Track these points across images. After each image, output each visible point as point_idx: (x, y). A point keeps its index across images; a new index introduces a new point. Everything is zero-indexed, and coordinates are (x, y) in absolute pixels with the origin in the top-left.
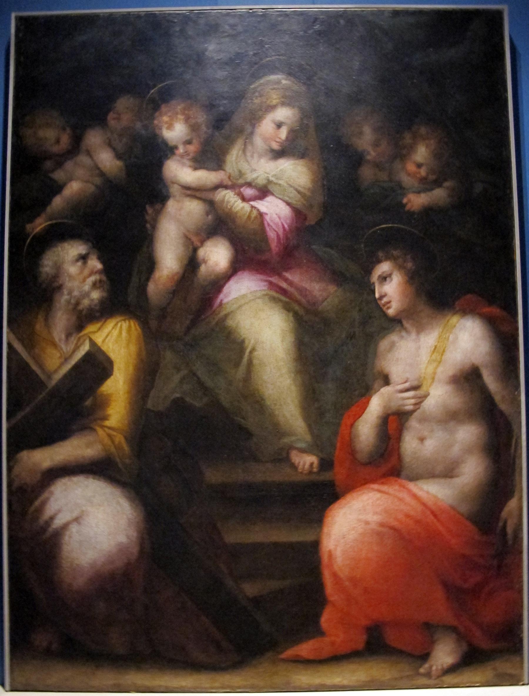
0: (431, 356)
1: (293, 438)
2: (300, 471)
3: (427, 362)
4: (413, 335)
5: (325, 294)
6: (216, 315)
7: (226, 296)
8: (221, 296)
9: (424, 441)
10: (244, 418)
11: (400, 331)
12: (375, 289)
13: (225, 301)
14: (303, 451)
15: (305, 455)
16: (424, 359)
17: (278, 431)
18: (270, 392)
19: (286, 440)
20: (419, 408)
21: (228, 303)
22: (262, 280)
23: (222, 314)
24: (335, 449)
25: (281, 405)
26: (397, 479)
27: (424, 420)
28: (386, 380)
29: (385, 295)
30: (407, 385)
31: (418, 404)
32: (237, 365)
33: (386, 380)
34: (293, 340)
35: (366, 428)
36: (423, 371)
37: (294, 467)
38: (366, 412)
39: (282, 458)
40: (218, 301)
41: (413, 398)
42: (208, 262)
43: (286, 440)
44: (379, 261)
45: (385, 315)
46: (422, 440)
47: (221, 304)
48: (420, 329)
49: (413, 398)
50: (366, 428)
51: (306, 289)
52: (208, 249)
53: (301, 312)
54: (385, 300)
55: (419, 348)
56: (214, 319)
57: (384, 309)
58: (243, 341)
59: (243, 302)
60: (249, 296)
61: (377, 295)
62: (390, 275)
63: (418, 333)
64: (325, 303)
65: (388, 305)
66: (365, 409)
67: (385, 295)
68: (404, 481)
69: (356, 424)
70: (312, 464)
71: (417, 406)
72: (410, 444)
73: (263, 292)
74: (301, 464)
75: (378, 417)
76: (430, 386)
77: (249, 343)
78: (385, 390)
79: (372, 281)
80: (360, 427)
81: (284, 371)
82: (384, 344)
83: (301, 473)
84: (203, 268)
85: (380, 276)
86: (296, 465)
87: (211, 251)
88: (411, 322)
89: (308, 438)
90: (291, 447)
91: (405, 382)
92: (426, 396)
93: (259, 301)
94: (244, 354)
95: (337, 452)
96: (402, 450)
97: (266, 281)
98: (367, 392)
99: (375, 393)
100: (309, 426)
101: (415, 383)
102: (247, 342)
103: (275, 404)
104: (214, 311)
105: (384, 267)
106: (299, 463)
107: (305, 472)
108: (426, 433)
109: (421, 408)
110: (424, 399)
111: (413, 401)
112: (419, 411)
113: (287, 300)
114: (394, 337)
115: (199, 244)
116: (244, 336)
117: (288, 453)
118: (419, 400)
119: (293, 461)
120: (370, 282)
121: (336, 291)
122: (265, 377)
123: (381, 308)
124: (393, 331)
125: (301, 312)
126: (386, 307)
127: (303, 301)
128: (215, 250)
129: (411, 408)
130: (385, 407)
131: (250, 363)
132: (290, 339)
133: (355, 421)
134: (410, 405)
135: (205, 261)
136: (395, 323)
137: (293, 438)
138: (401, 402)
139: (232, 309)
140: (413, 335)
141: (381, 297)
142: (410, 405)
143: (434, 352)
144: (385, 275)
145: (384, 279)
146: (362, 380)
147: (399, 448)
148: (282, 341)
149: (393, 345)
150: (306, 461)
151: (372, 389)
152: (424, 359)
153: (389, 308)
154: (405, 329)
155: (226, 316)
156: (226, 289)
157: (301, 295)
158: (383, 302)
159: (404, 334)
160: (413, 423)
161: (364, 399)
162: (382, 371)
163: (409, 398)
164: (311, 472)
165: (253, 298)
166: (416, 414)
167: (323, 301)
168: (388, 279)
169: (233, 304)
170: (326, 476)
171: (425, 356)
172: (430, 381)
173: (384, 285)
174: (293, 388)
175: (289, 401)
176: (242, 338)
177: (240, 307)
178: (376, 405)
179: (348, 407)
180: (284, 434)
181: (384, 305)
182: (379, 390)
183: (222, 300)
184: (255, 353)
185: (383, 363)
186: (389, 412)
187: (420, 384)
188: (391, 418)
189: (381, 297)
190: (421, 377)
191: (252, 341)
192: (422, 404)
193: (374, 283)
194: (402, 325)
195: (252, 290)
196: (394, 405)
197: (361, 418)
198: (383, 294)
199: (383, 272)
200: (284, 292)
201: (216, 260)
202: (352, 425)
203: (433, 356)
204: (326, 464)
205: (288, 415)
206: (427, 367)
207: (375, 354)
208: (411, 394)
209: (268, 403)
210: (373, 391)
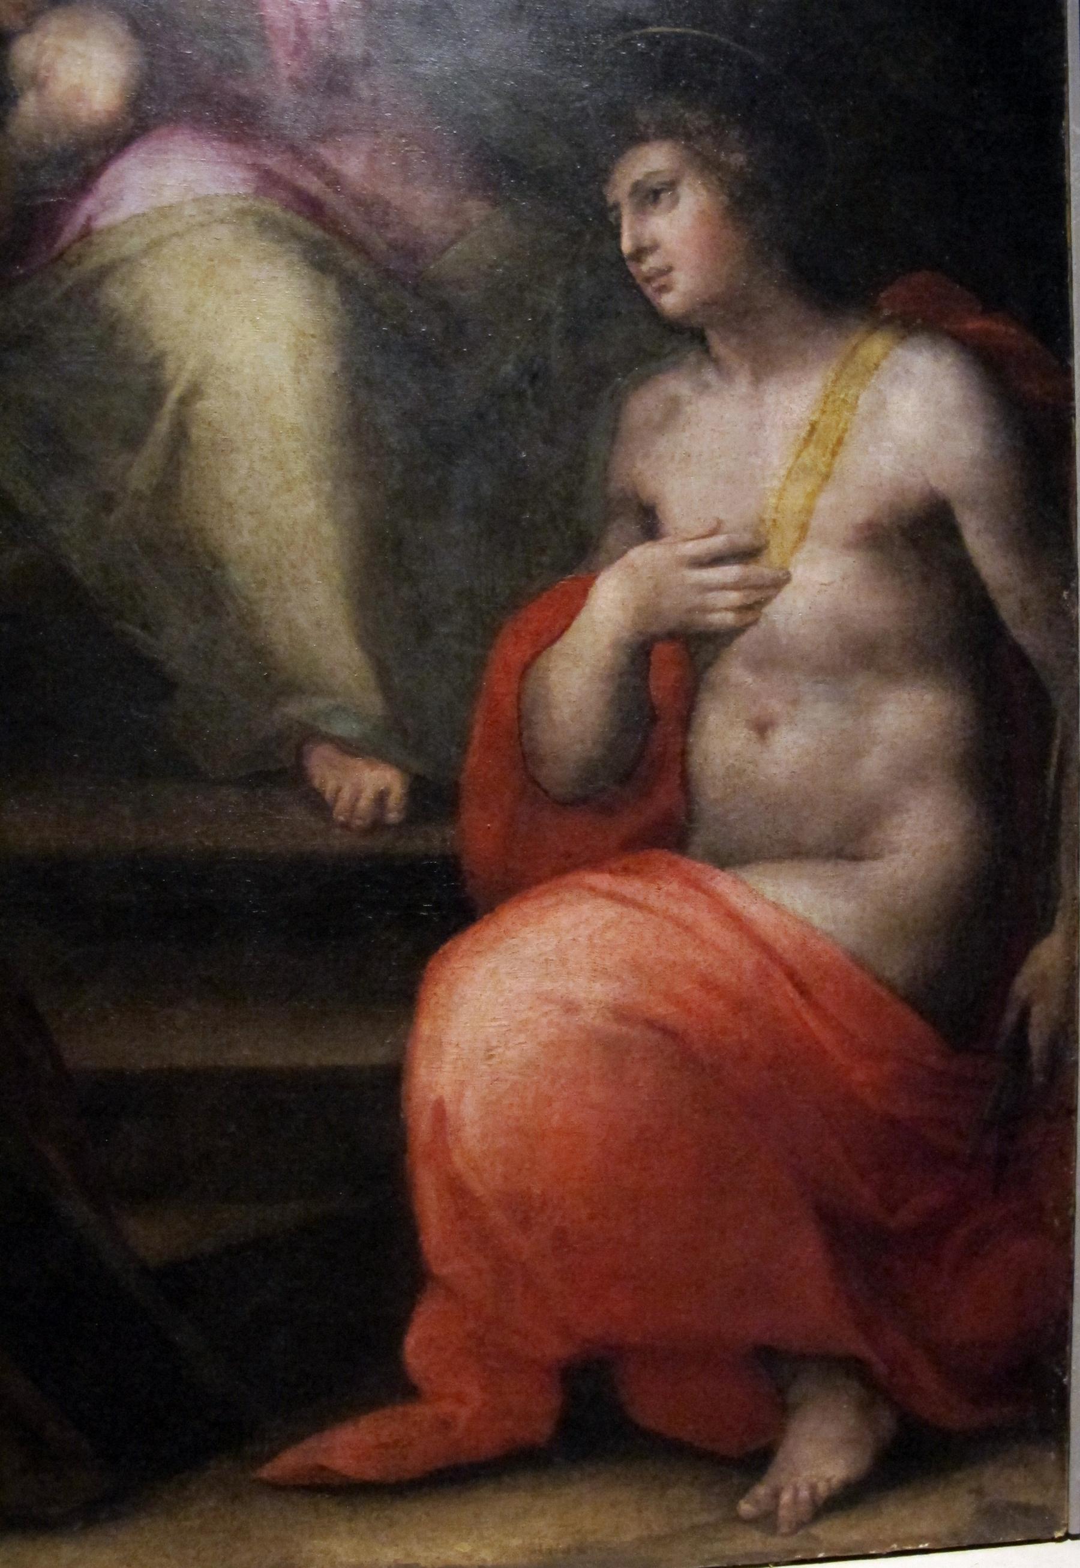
0: (798, 457)
1: (321, 703)
2: (341, 818)
3: (783, 472)
4: (742, 384)
5: (452, 225)
6: (71, 266)
7: (105, 208)
8: (89, 205)
9: (770, 732)
10: (144, 626)
11: (700, 364)
12: (619, 226)
13: (103, 221)
14: (348, 748)
15: (359, 763)
16: (775, 461)
17: (272, 678)
18: (246, 538)
19: (294, 709)
20: (755, 622)
21: (110, 230)
22: (236, 162)
23: (93, 262)
24: (464, 746)
25: (282, 587)
26: (675, 857)
27: (771, 661)
28: (649, 523)
29: (654, 247)
30: (717, 542)
31: (751, 610)
32: (133, 440)
33: (649, 523)
34: (333, 367)
35: (576, 674)
36: (773, 501)
37: (319, 804)
38: (575, 624)
39: (279, 771)
40: (80, 219)
41: (735, 587)
42: (51, 85)
43: (294, 709)
44: (638, 139)
45: (653, 313)
46: (762, 728)
47: (86, 233)
48: (765, 364)
49: (735, 587)
50: (576, 674)
51: (388, 204)
52: (50, 41)
53: (367, 277)
54: (651, 263)
55: (761, 425)
56: (59, 280)
57: (649, 290)
58: (157, 363)
59: (166, 228)
60: (189, 210)
61: (627, 245)
62: (672, 185)
63: (757, 379)
64: (450, 255)
65: (662, 281)
66: (572, 615)
67: (654, 247)
68: (699, 865)
69: (542, 661)
70: (381, 798)
71: (749, 617)
72: (721, 740)
73: (239, 204)
74: (346, 794)
75: (615, 645)
76: (792, 554)
77: (179, 369)
78: (642, 555)
79: (611, 200)
80: (554, 676)
81: (299, 467)
82: (643, 405)
83: (345, 826)
84: (29, 105)
85: (636, 187)
86: (328, 796)
87: (60, 50)
88: (734, 341)
89: (374, 703)
90: (308, 735)
91: (713, 533)
92: (779, 583)
93: (223, 232)
94: (161, 405)
95: (472, 760)
96: (696, 759)
97: (254, 166)
98: (579, 556)
99: (611, 561)
100: (382, 671)
101: (745, 539)
102: (171, 364)
103: (262, 584)
104: (61, 254)
105: (654, 159)
106: (339, 790)
107: (359, 822)
108: (776, 706)
109: (763, 624)
110: (771, 592)
111: (734, 597)
112: (753, 633)
113: (318, 234)
114: (676, 384)
115: (20, 24)
116: (160, 345)
117: (299, 755)
118: (756, 596)
119: (316, 783)
120: (603, 198)
121: (487, 220)
122: (231, 490)
123: (637, 287)
124: (676, 365)
125: (367, 277)
126: (655, 285)
127: (378, 243)
128: (79, 46)
129: (730, 618)
130: (639, 610)
131: (180, 434)
132: (324, 362)
133: (537, 655)
134: (727, 609)
135: (38, 82)
136: (684, 339)
137: (321, 703)
138: (697, 600)
139: (125, 251)
140: (742, 384)
141: (640, 253)
142: (727, 609)
143: (807, 441)
144: (654, 183)
145: (650, 195)
146: (569, 519)
147: (684, 753)
148: (296, 371)
149: (673, 408)
150: (364, 785)
151: (597, 548)
152: (775, 461)
153: (664, 289)
154: (716, 362)
155: (104, 272)
156: (106, 184)
157: (370, 223)
158: (644, 268)
159: (710, 375)
160: (734, 671)
161: (566, 582)
162: (636, 495)
163: (724, 587)
164: (377, 825)
165: (199, 219)
166: (743, 641)
167: (445, 250)
168: (663, 196)
169: (132, 234)
170: (431, 840)
171: (777, 450)
172: (792, 535)
173: (652, 213)
174: (327, 529)
175: (310, 572)
176: (151, 353)
177: (155, 246)
178: (610, 603)
179: (515, 602)
180: (291, 689)
181: (648, 280)
182: (624, 553)
183: (89, 219)
184: (200, 405)
185: (640, 465)
186: (655, 629)
187: (757, 543)
188: (658, 646)
189: (640, 253)
190: (762, 521)
191: (192, 363)
192: (766, 610)
193: (616, 206)
194: (707, 350)
195: (201, 192)
196: (673, 608)
197: (557, 646)
198: (647, 243)
199: (649, 175)
200: (312, 208)
201: (76, 81)
202: (526, 668)
203: (804, 454)
204: (433, 797)
205: (303, 620)
206: (781, 493)
207: (613, 434)
208: (730, 572)
209: (237, 576)
210: (603, 557)
